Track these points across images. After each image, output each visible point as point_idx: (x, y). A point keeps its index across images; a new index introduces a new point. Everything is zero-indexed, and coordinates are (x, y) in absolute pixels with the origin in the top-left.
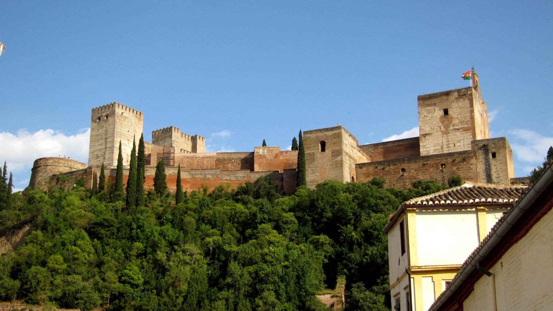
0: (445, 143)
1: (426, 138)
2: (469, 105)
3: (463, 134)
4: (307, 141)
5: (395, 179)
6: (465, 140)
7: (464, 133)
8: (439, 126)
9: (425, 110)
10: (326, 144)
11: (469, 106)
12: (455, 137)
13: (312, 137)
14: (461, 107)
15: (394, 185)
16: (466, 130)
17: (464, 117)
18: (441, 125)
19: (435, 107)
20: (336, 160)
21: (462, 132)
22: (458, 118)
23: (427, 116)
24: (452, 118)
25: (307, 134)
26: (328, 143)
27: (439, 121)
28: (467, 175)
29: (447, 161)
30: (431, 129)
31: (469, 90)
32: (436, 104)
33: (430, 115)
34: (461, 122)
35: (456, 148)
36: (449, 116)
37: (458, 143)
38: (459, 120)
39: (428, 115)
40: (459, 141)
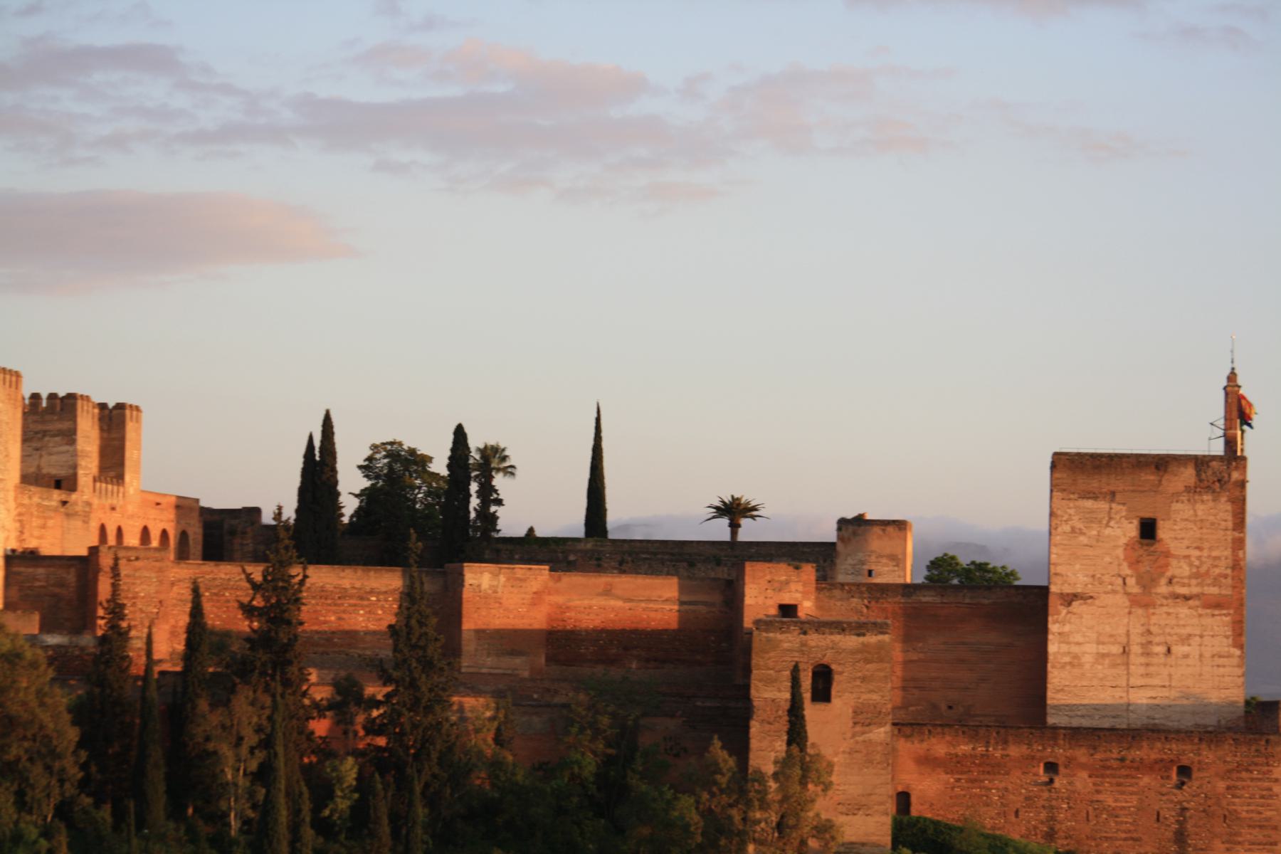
0: (1136, 639)
1: (1070, 609)
2: (1230, 518)
3: (1200, 615)
4: (767, 656)
5: (1021, 793)
6: (1207, 640)
7: (1207, 614)
8: (1120, 576)
9: (1076, 507)
10: (836, 678)
11: (1230, 525)
12: (1174, 622)
13: (786, 645)
14: (1202, 521)
15: (1017, 813)
16: (1216, 604)
17: (1209, 557)
18: (1128, 572)
19: (1114, 505)
20: (867, 737)
21: (1200, 611)
22: (1187, 557)
23: (1082, 533)
24: (1167, 554)
25: (767, 631)
26: (841, 673)
27: (1122, 557)
28: (1260, 813)
29: (1197, 758)
30: (1091, 580)
31: (1236, 468)
32: (1118, 497)
33: (1095, 533)
34: (1197, 575)
35: (1171, 660)
36: (1157, 545)
37: (1183, 645)
38: (1191, 565)
39: (1085, 530)
40: (1186, 639)
